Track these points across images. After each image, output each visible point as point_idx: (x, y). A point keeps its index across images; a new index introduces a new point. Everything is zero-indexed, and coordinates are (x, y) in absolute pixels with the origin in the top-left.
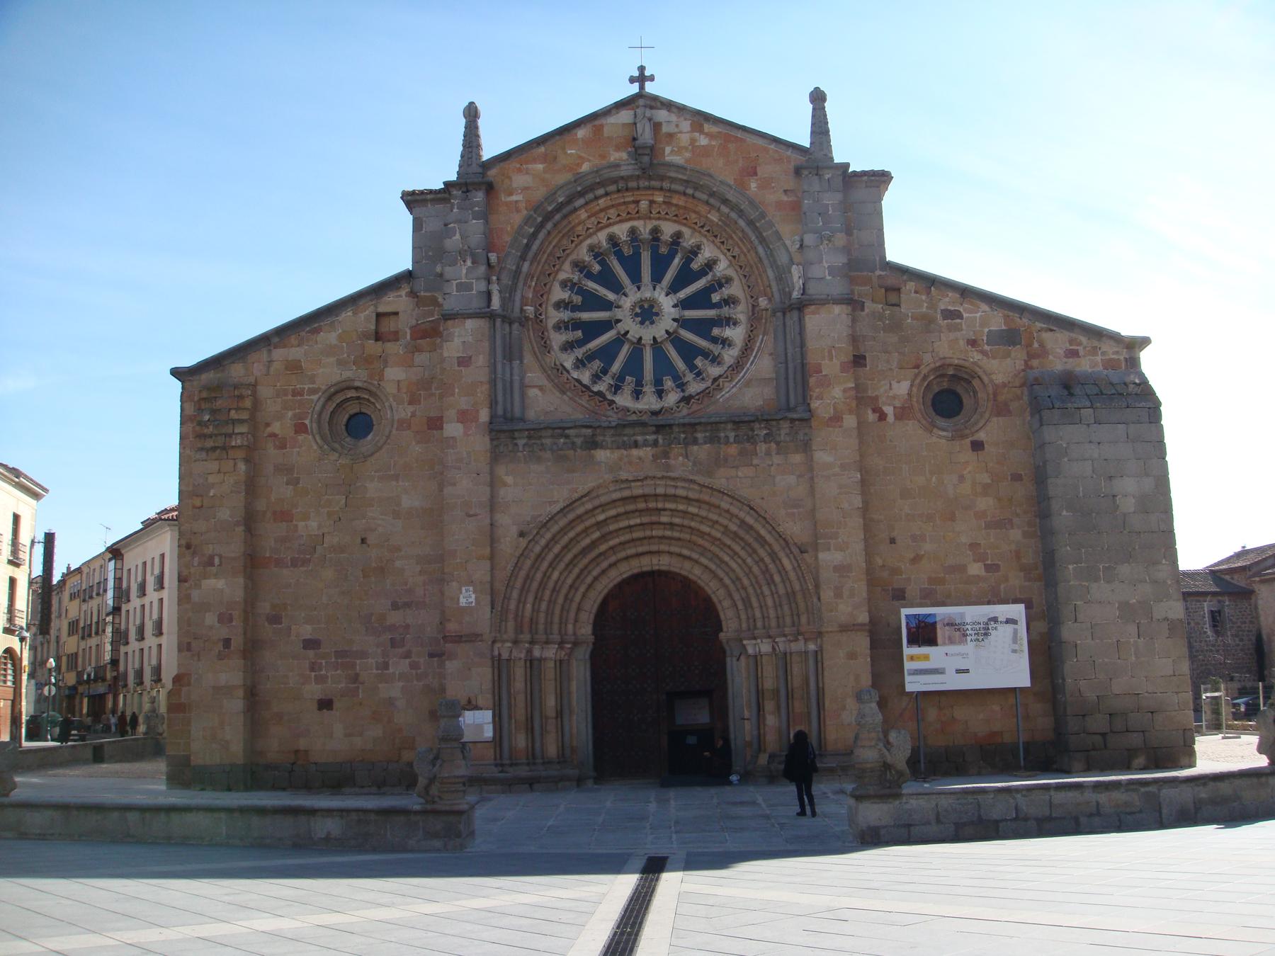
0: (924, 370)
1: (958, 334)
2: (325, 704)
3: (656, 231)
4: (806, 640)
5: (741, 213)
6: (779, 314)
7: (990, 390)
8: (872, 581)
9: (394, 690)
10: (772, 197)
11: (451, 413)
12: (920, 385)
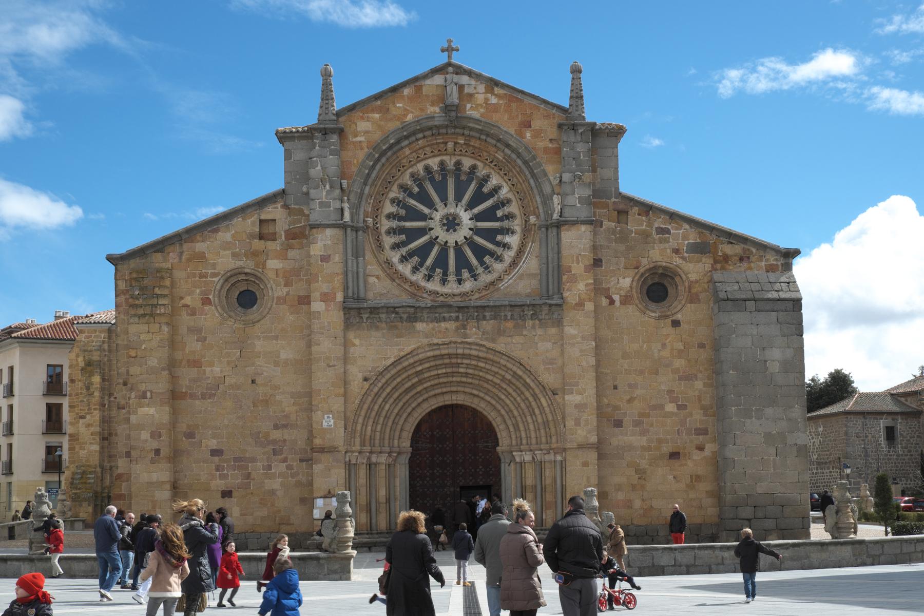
0: (642, 270)
1: (667, 245)
3: (458, 164)
4: (555, 453)
5: (519, 155)
7: (687, 284)
9: (275, 484)
11: (316, 295)
12: (639, 280)
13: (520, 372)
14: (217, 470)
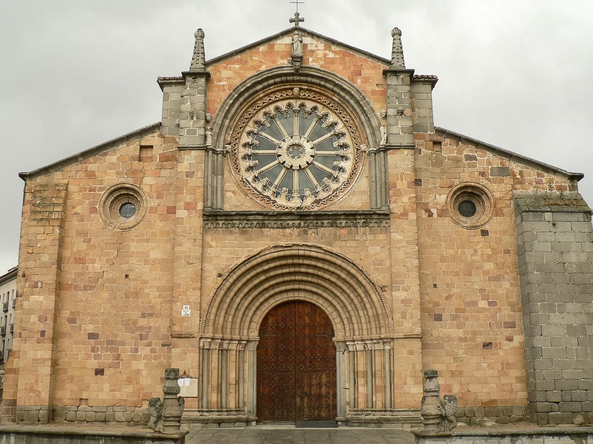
0: (455, 189)
1: (474, 169)
2: (99, 372)
3: (302, 105)
4: (384, 343)
5: (352, 96)
6: (373, 155)
8: (423, 310)
9: (140, 365)
10: (369, 88)
13: (353, 271)
14: (93, 351)
